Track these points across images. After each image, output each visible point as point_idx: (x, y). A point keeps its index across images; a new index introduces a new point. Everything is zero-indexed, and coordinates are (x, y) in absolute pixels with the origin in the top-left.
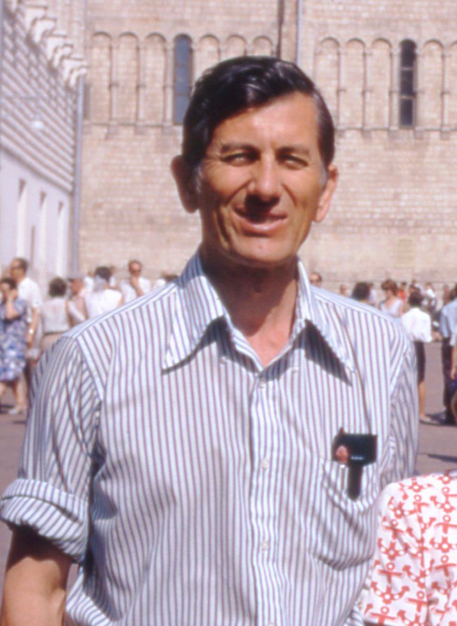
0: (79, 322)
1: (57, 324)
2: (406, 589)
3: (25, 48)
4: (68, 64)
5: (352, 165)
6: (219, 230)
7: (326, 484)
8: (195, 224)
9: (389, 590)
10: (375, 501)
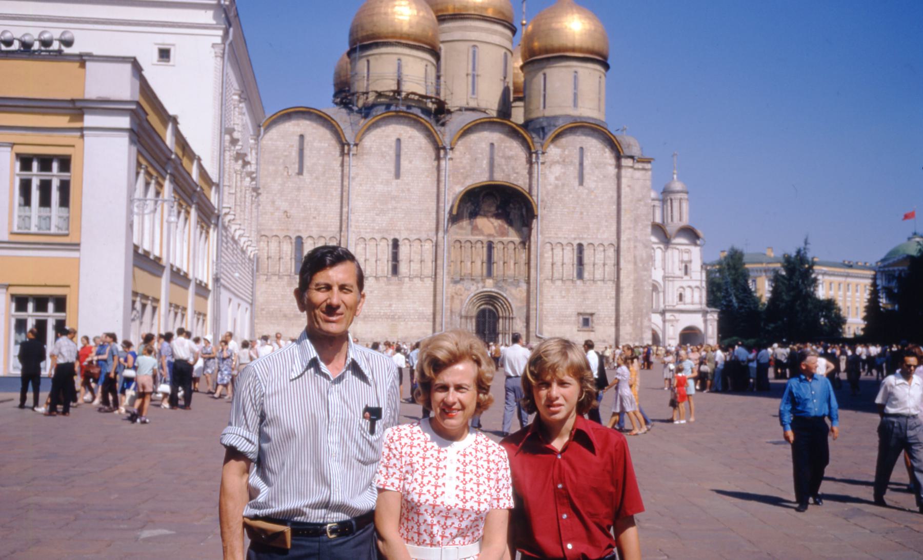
0: (254, 359)
1: (245, 360)
3: (232, 242)
4: (250, 249)
5: (371, 292)
6: (314, 320)
7: (360, 429)
8: (304, 317)
9: (387, 474)
10: (381, 436)
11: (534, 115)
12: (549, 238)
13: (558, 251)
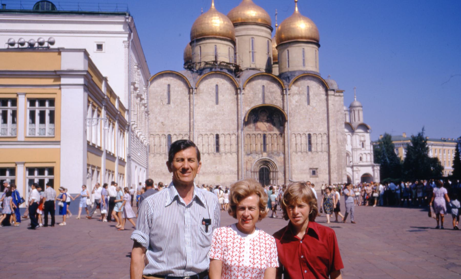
2: (218, 251)
3: (136, 138)
4: (145, 141)
9: (215, 251)
11: (284, 71)
12: (294, 131)
13: (299, 138)
